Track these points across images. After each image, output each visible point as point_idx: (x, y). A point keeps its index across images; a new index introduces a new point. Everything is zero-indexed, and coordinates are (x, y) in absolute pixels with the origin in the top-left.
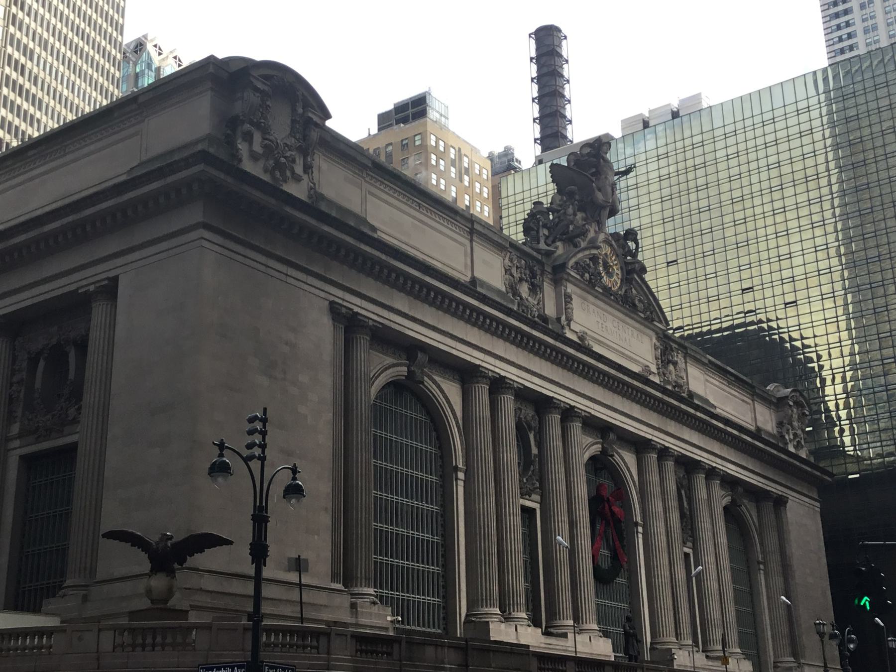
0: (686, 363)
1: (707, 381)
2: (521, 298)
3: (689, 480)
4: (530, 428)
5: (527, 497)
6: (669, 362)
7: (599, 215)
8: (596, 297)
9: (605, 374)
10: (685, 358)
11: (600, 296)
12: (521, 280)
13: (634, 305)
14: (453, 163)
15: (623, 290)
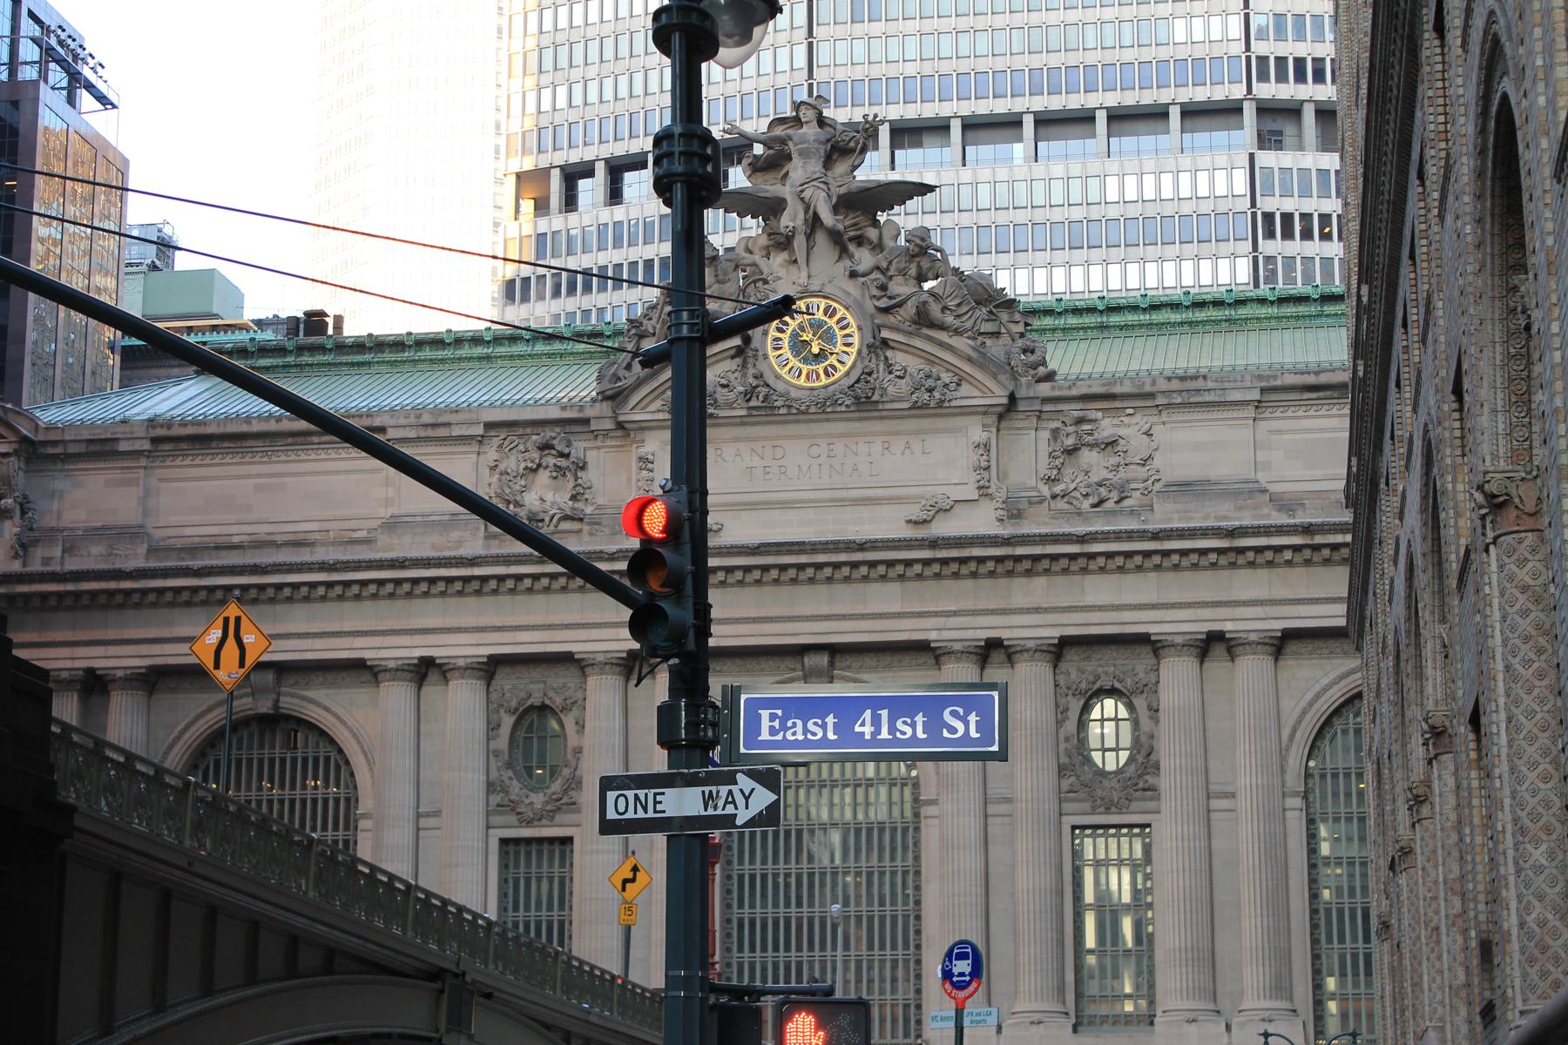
1: (1280, 432)
4: (564, 709)
5: (544, 822)
8: (744, 424)
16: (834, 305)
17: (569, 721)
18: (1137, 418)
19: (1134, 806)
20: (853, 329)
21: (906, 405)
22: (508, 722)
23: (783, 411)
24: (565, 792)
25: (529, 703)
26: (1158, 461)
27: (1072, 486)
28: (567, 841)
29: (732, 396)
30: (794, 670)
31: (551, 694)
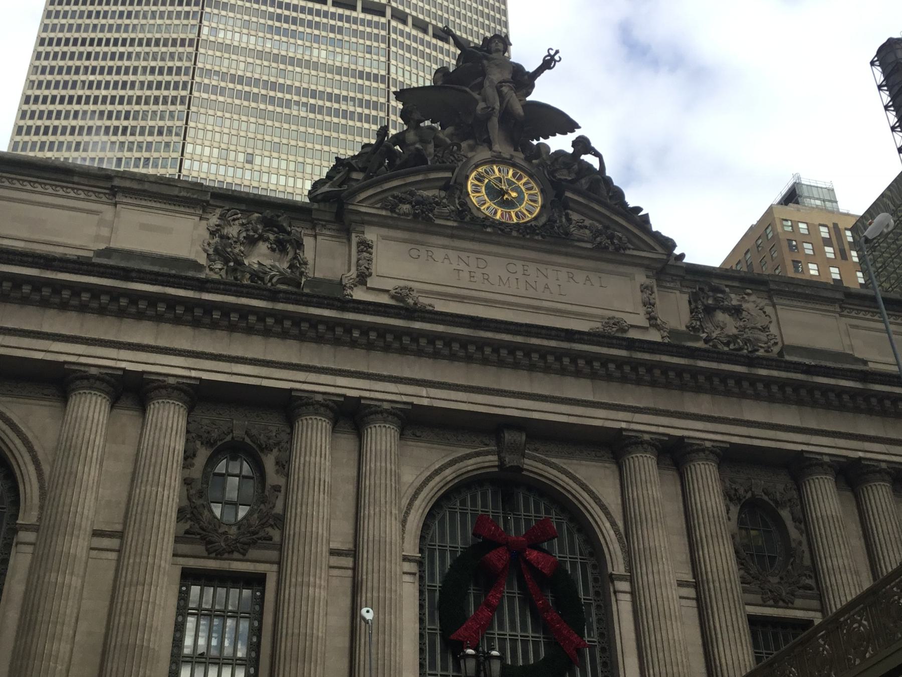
0: (774, 306)
1: (856, 327)
2: (240, 263)
3: (799, 489)
4: (267, 449)
5: (236, 555)
6: (709, 311)
7: (488, 132)
8: (452, 236)
9: (449, 340)
10: (770, 298)
11: (455, 232)
12: (252, 242)
13: (567, 234)
14: (827, 242)
15: (543, 220)
16: (520, 173)
17: (269, 462)
18: (753, 298)
19: (798, 602)
20: (536, 190)
21: (589, 246)
22: (203, 454)
23: (489, 230)
24: (263, 525)
25: (229, 438)
26: (773, 330)
27: (714, 335)
28: (256, 581)
29: (446, 210)
30: (487, 445)
31: (254, 432)
